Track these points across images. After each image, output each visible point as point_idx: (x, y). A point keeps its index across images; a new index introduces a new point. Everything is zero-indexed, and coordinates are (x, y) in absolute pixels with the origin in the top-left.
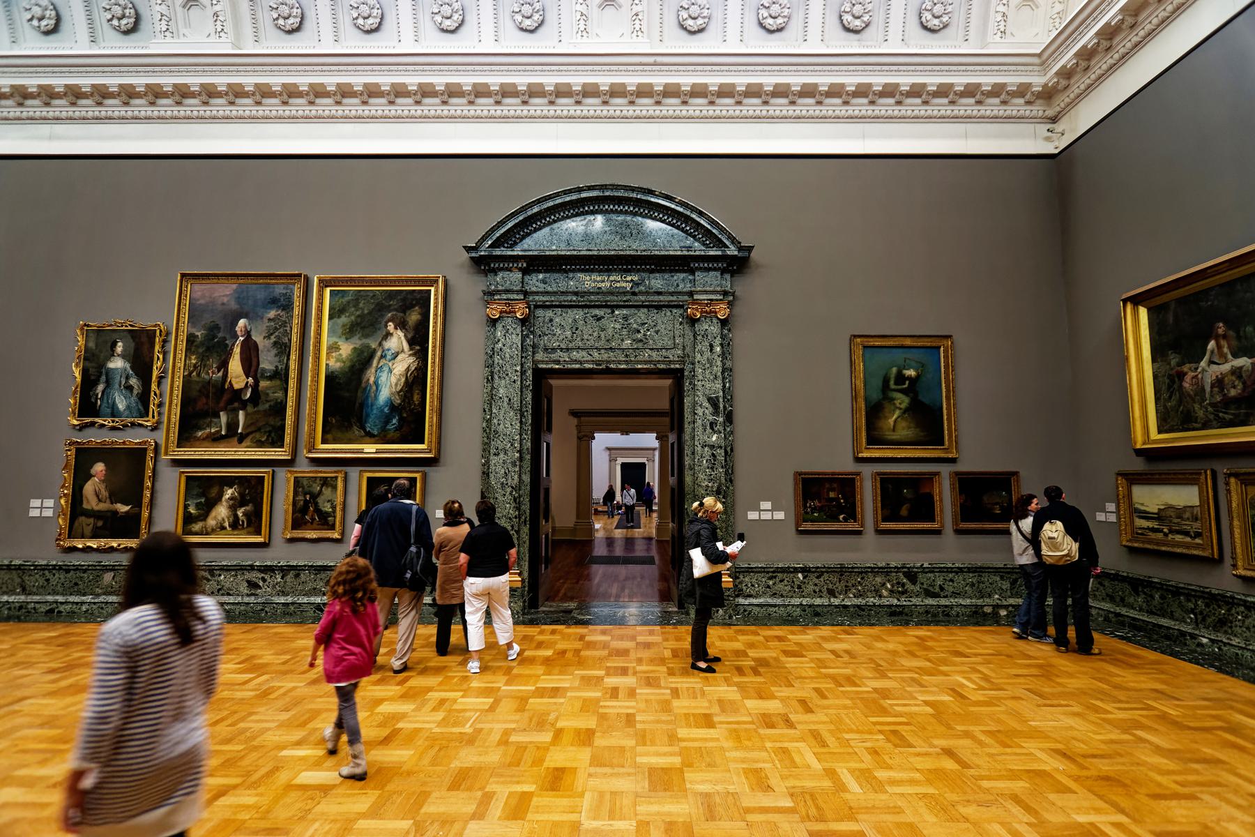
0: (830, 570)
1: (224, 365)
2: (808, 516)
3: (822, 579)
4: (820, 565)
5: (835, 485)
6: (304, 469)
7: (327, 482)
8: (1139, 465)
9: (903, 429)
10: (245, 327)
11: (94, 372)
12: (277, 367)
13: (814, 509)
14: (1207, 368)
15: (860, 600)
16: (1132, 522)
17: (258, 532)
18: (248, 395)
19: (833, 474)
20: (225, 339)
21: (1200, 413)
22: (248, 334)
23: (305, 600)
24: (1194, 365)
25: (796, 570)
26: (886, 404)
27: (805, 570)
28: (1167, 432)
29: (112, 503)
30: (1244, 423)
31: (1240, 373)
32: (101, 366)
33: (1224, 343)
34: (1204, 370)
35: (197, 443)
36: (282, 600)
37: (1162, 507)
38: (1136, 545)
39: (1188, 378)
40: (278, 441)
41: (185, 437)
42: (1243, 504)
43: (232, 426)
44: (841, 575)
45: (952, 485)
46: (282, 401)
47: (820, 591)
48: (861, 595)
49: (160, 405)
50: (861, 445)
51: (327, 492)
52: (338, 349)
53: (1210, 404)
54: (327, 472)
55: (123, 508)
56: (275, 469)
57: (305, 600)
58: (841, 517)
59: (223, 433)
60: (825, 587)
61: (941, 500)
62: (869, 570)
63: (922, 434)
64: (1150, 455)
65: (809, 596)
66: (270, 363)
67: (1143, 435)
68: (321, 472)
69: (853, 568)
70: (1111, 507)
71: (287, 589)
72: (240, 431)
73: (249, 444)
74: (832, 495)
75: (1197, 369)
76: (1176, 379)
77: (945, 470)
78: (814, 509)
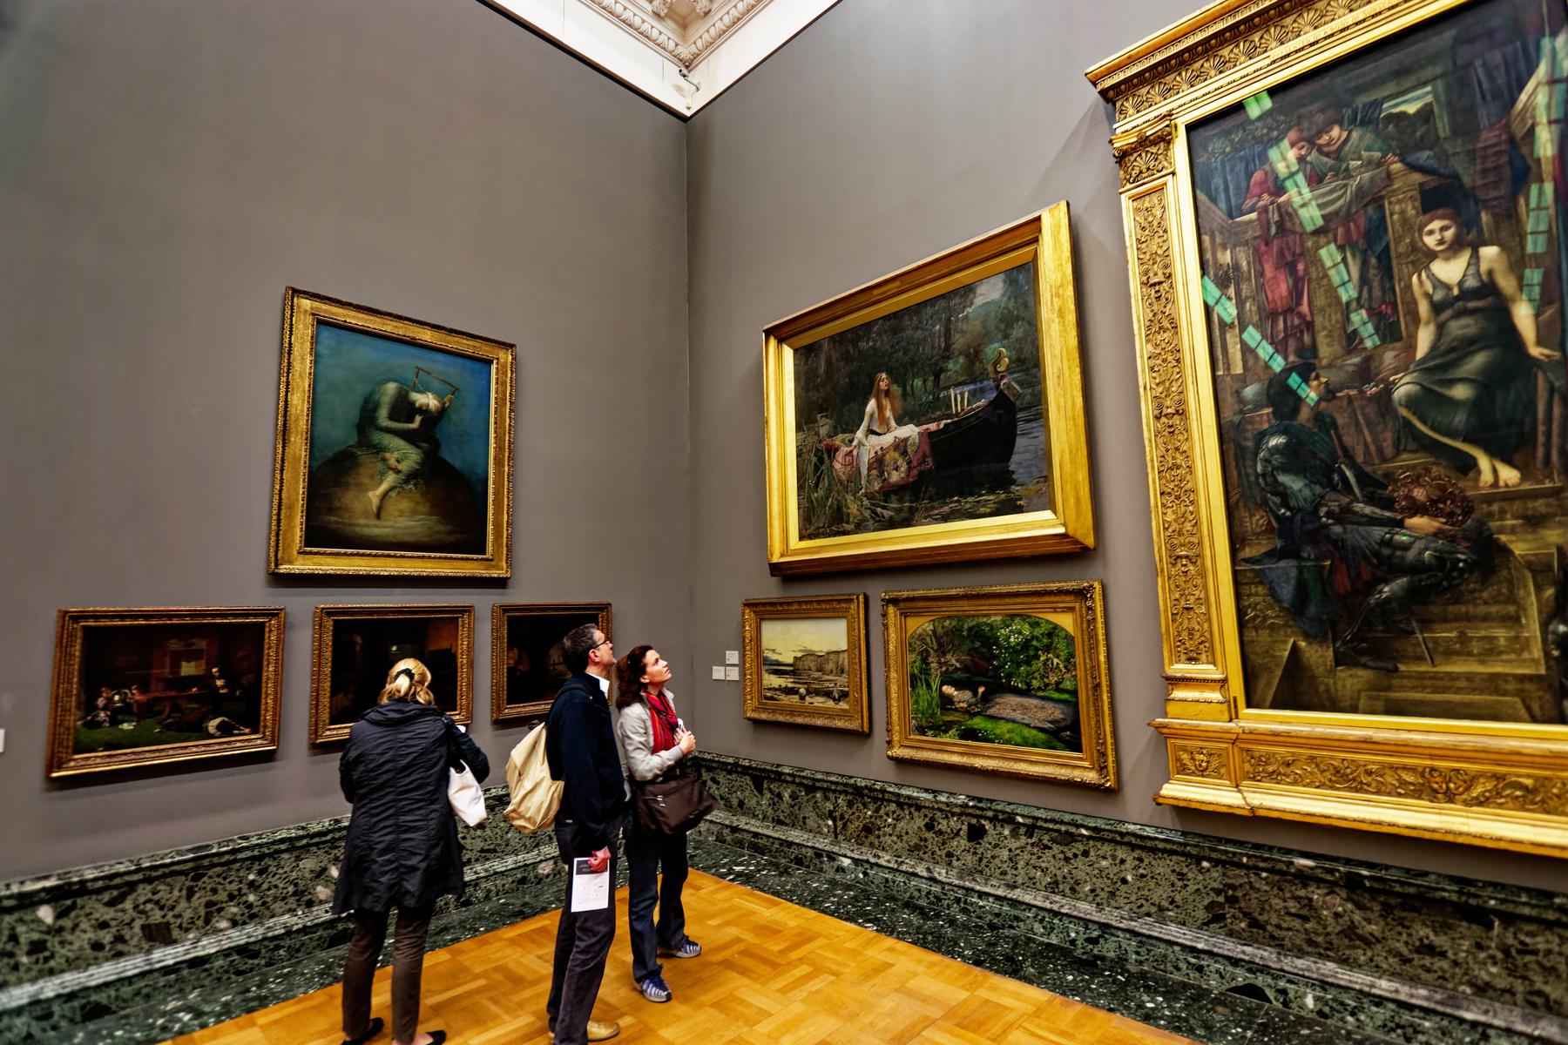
0: (154, 875)
2: (98, 735)
3: (128, 905)
4: (122, 868)
5: (202, 644)
8: (770, 589)
9: (402, 514)
13: (126, 711)
14: (864, 441)
15: (249, 929)
16: (760, 680)
19: (194, 614)
21: (853, 509)
24: (848, 436)
25: (27, 901)
26: (364, 457)
27: (66, 896)
28: (811, 537)
30: (907, 523)
31: (906, 446)
33: (886, 403)
34: (860, 444)
37: (799, 655)
38: (764, 716)
39: (840, 456)
42: (902, 640)
44: (197, 878)
45: (495, 629)
47: (119, 939)
48: (252, 917)
50: (288, 547)
53: (866, 495)
58: (213, 725)
60: (137, 924)
61: (471, 664)
62: (283, 847)
63: (442, 528)
64: (787, 573)
65: (72, 964)
67: (782, 542)
69: (233, 852)
70: (733, 657)
74: (188, 669)
75: (851, 441)
76: (826, 456)
77: (484, 602)
78: (126, 711)
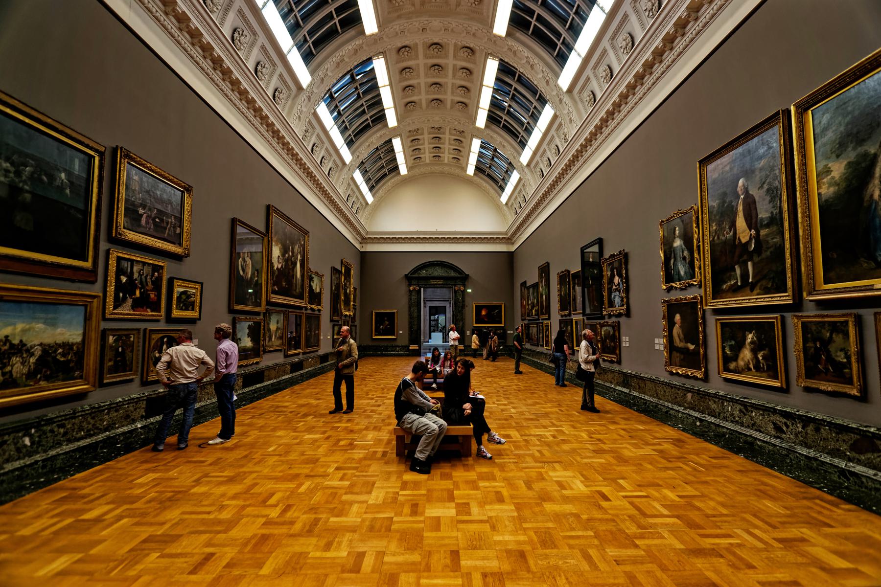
1: (733, 225)
6: (811, 313)
7: (840, 328)
10: (744, 185)
11: (669, 253)
12: (772, 213)
17: (775, 377)
18: (753, 246)
20: (731, 202)
22: (746, 191)
23: (827, 459)
29: (687, 342)
32: (671, 246)
35: (724, 295)
36: (804, 451)
40: (781, 288)
41: (717, 293)
43: (745, 275)
46: (780, 245)
49: (700, 269)
51: (838, 339)
52: (828, 171)
54: (835, 316)
55: (692, 347)
56: (785, 314)
57: (827, 459)
59: (739, 284)
66: (766, 211)
68: (827, 316)
71: (809, 441)
72: (750, 280)
73: (758, 291)
